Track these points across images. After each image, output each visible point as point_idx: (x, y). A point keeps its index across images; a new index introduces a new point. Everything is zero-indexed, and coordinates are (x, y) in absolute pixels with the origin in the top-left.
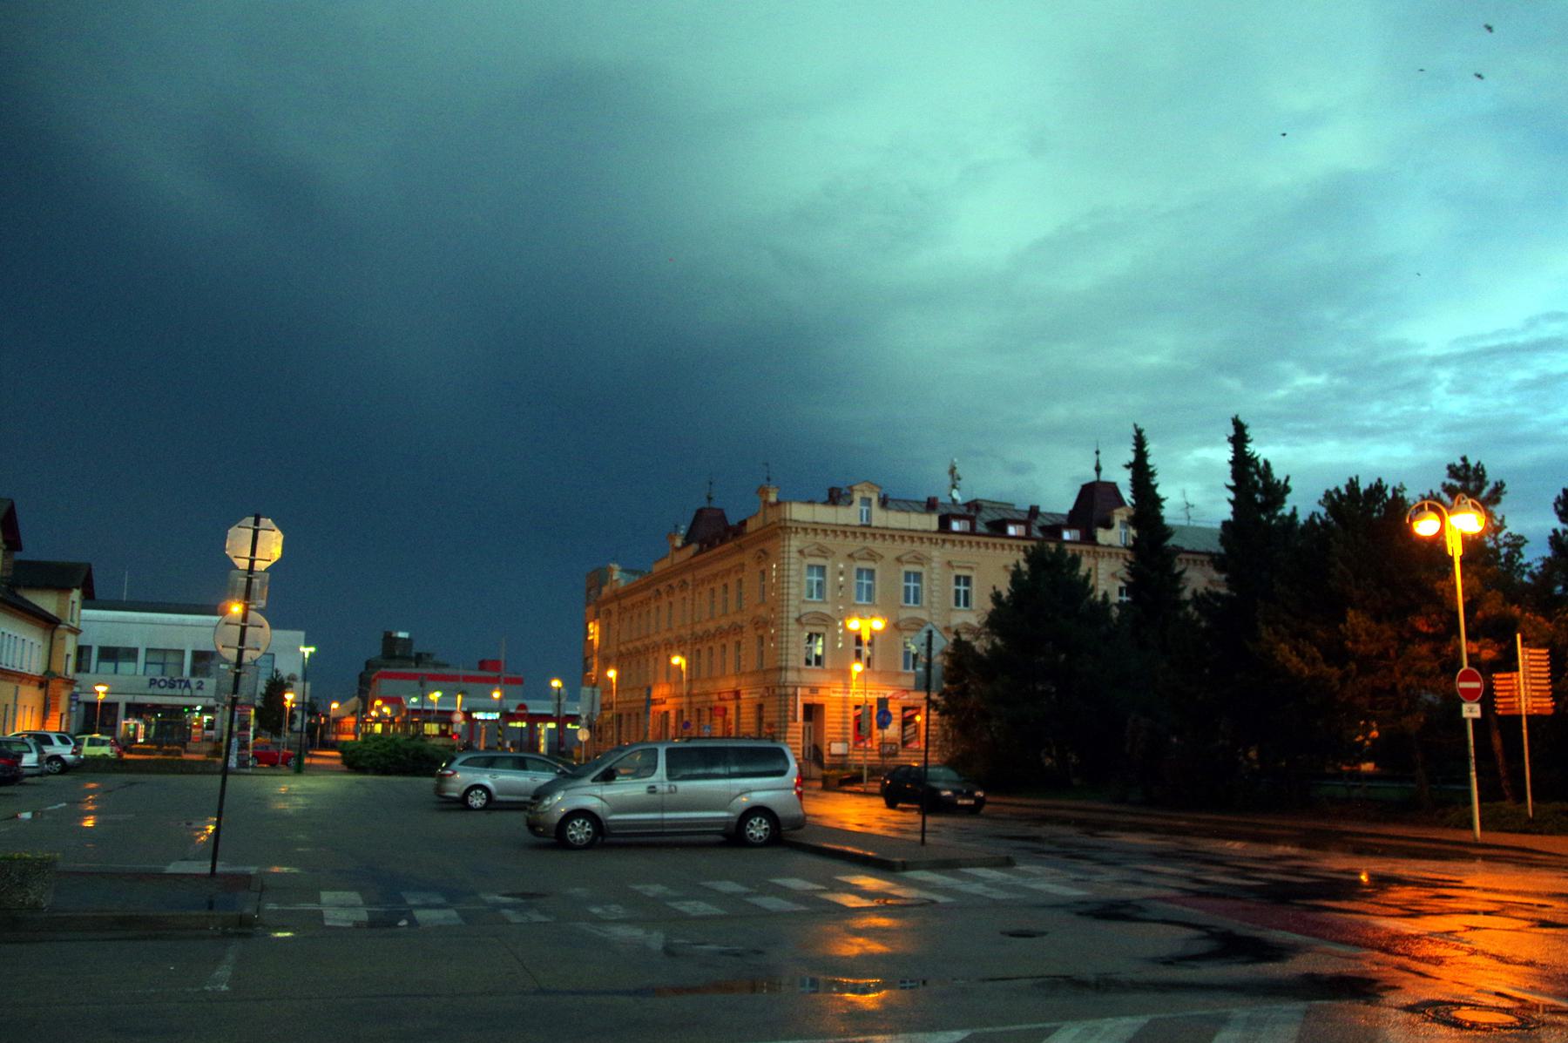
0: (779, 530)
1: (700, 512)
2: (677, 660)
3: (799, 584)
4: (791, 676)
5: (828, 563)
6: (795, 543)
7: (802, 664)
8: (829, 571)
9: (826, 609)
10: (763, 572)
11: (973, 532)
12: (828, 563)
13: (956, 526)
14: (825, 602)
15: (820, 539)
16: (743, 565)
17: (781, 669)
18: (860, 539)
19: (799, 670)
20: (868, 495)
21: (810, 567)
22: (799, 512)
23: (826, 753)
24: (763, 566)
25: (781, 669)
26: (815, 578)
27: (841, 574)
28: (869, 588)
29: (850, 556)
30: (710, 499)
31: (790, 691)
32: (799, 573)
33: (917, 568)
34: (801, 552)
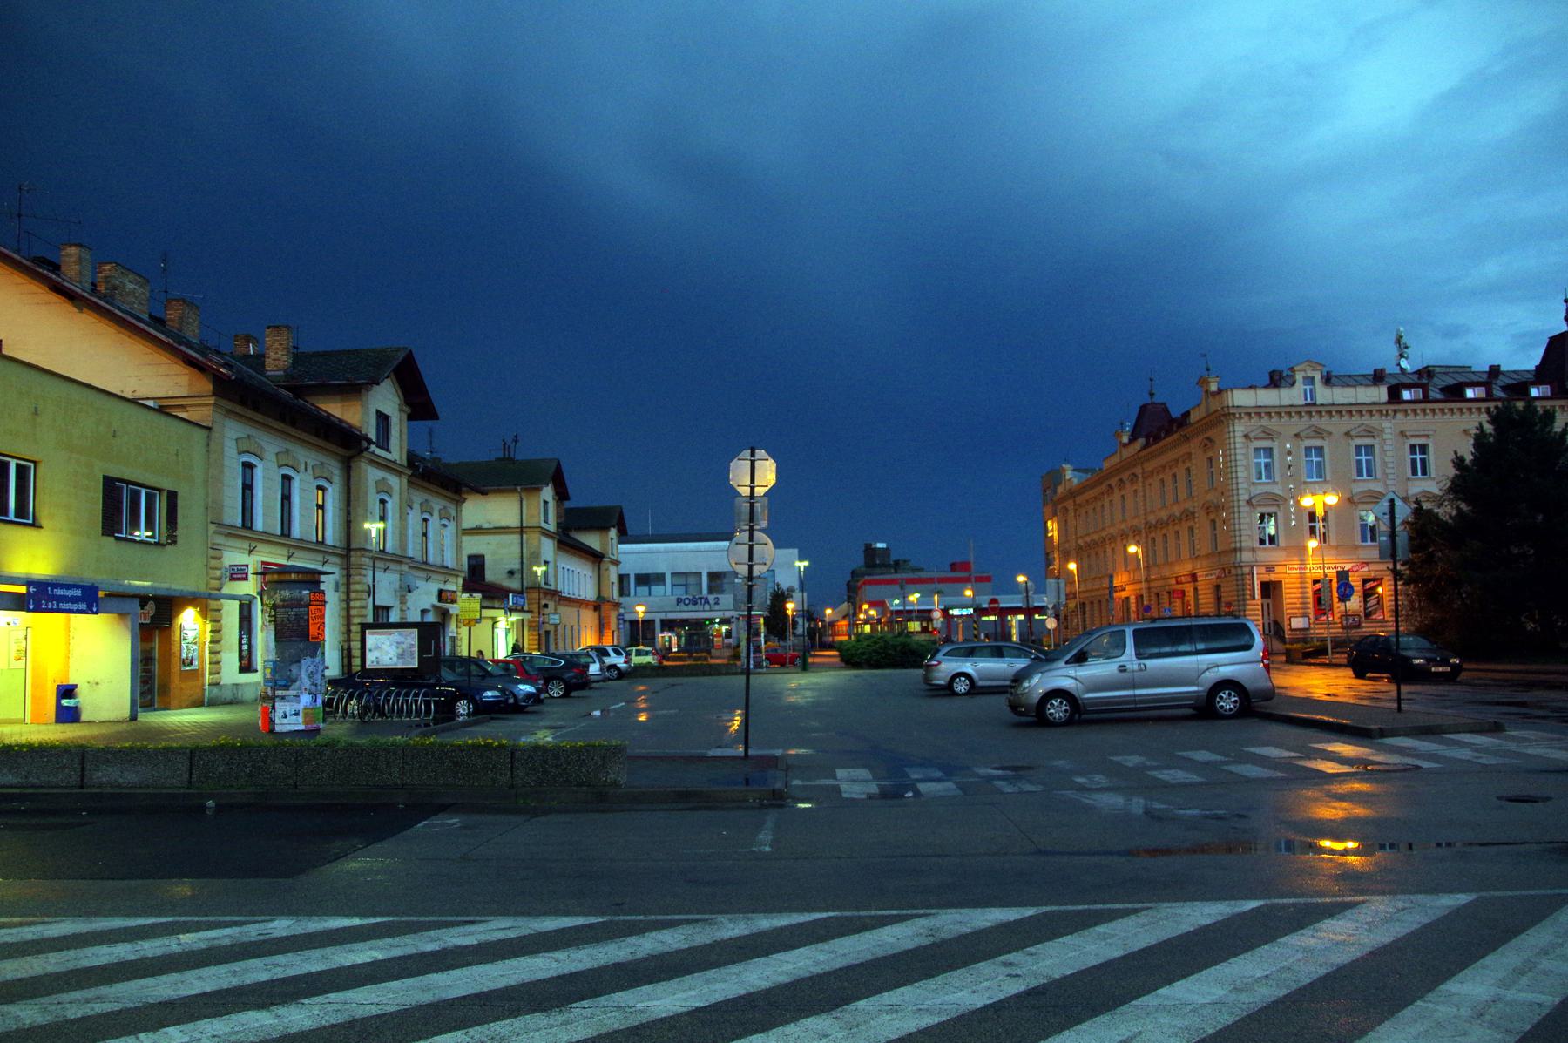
0: (1224, 416)
1: (1143, 408)
2: (1132, 549)
3: (1247, 468)
4: (1246, 557)
5: (1275, 445)
6: (1239, 428)
7: (1257, 544)
8: (1275, 452)
9: (1277, 490)
10: (1210, 459)
11: (1426, 399)
12: (1275, 445)
13: (1406, 395)
14: (1275, 483)
15: (1265, 421)
16: (1190, 454)
17: (1235, 550)
18: (1306, 418)
19: (1253, 550)
20: (1310, 374)
21: (1257, 450)
22: (1241, 398)
23: (1286, 628)
24: (1210, 454)
25: (1235, 550)
26: (1263, 461)
27: (1289, 453)
28: (1319, 465)
29: (1297, 435)
30: (1152, 395)
31: (1247, 570)
32: (1246, 455)
33: (1368, 441)
34: (1246, 436)
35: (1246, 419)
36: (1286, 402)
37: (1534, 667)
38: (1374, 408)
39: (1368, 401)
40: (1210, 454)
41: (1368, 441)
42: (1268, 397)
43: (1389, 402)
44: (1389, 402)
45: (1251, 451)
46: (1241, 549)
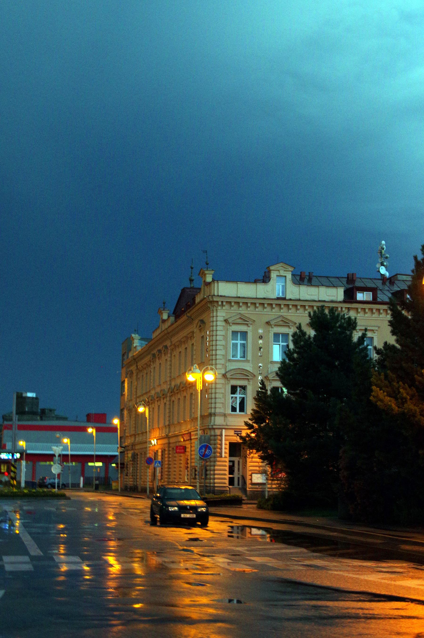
0: (211, 303)
1: (183, 291)
2: (141, 409)
3: (225, 347)
4: (219, 421)
5: (249, 330)
6: (221, 313)
7: (229, 411)
8: (250, 336)
9: (248, 367)
10: (203, 337)
11: (375, 301)
12: (249, 330)
13: (360, 296)
14: (248, 361)
15: (243, 310)
16: (193, 332)
17: (210, 415)
18: (276, 309)
19: (225, 415)
20: (282, 273)
21: (235, 333)
22: (225, 289)
23: (248, 482)
24: (203, 334)
25: (210, 415)
26: (239, 342)
27: (261, 337)
28: (244, 346)
29: (268, 323)
30: (191, 280)
31: (218, 432)
32: (225, 337)
33: (243, 328)
34: (226, 321)
35: (227, 307)
36: (261, 295)
37: (356, 529)
38: (249, 301)
39: (308, 298)
40: (203, 334)
41: (243, 328)
42: (246, 290)
43: (344, 302)
44: (344, 302)
45: (230, 334)
46: (215, 414)
